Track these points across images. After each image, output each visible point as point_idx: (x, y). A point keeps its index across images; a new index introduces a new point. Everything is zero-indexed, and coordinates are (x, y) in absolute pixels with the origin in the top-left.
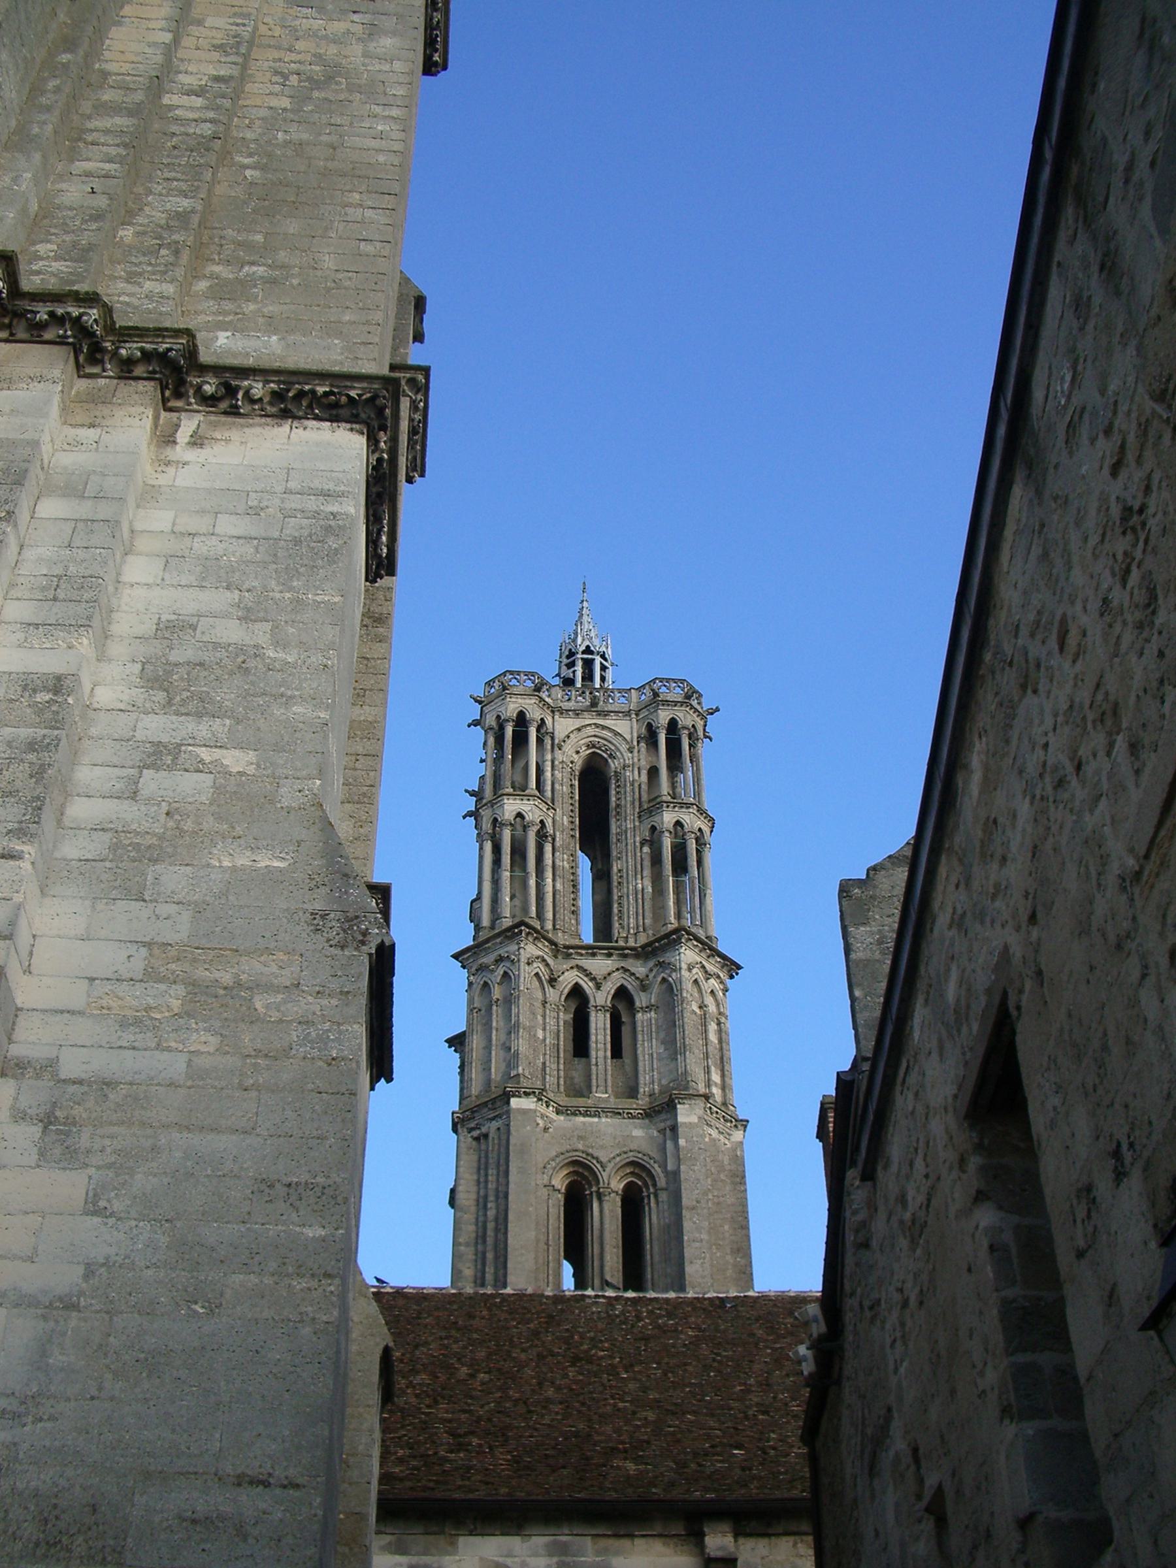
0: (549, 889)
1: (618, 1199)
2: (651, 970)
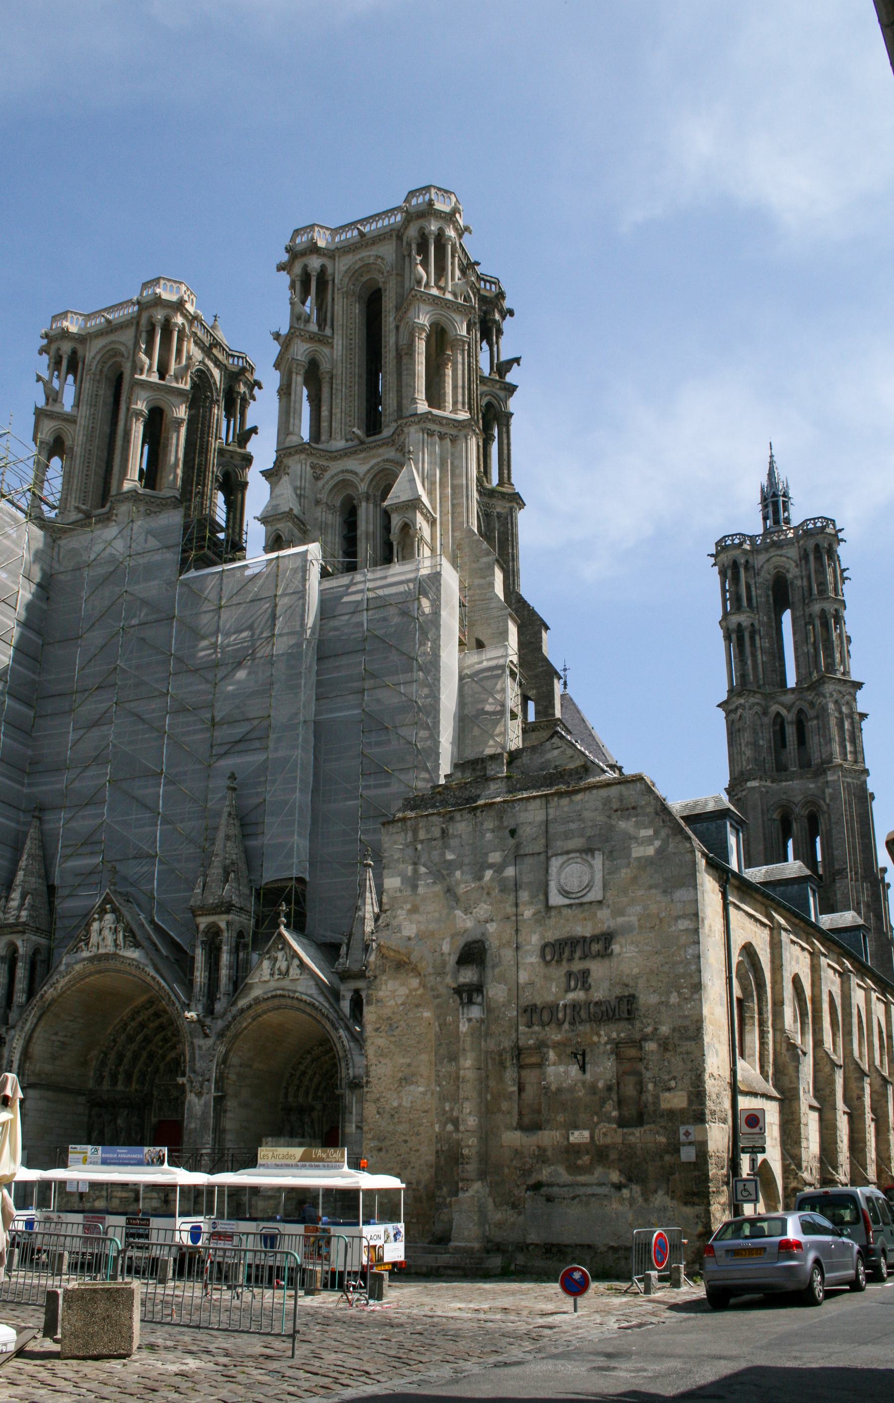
0: (760, 661)
1: (806, 820)
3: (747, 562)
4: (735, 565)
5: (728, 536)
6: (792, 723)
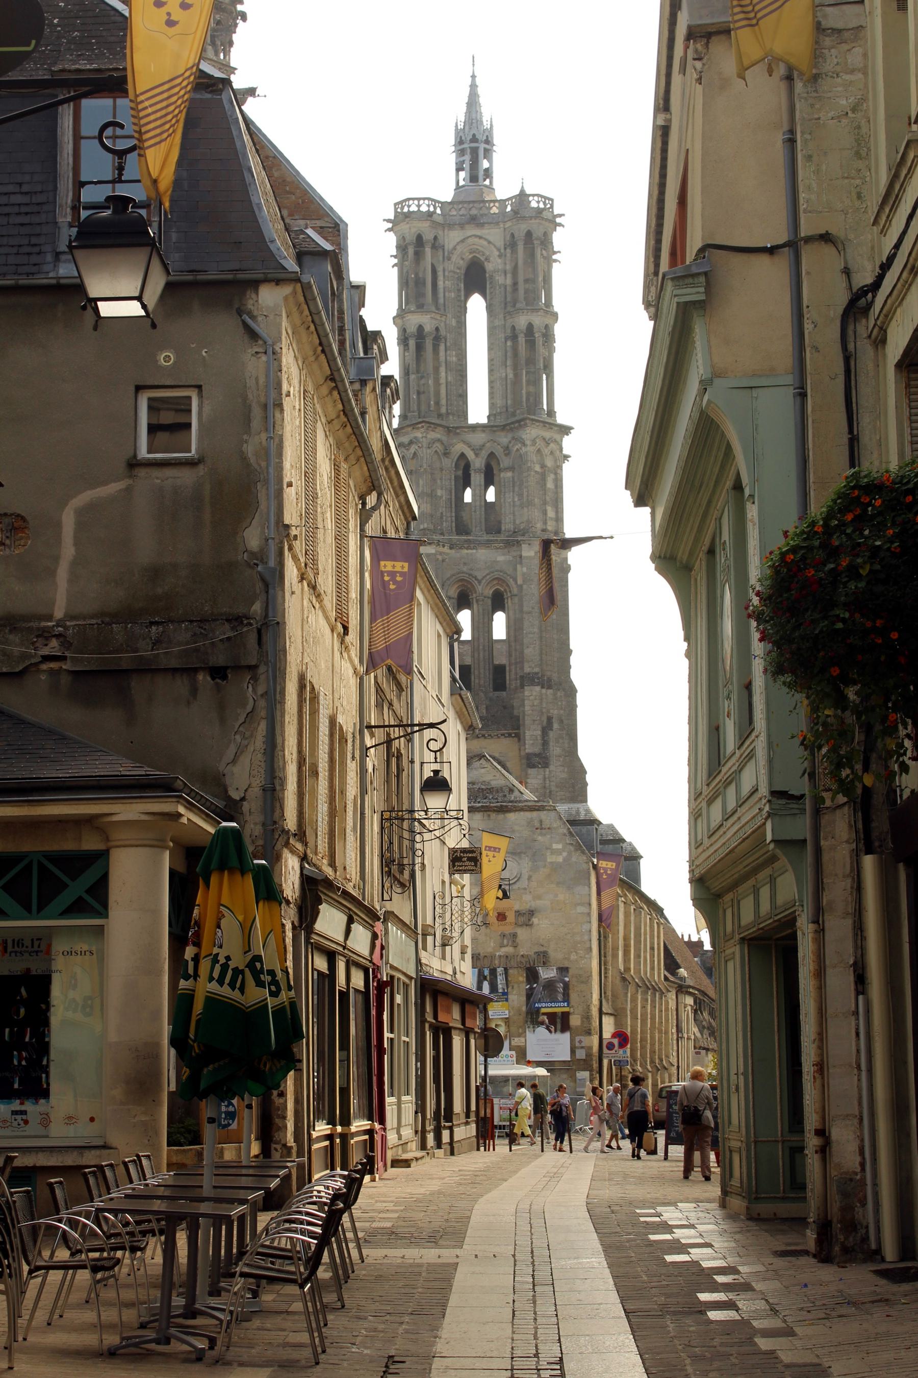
0: (443, 381)
2: (510, 442)
3: (435, 238)
4: (420, 240)
5: (413, 199)
6: (478, 471)
